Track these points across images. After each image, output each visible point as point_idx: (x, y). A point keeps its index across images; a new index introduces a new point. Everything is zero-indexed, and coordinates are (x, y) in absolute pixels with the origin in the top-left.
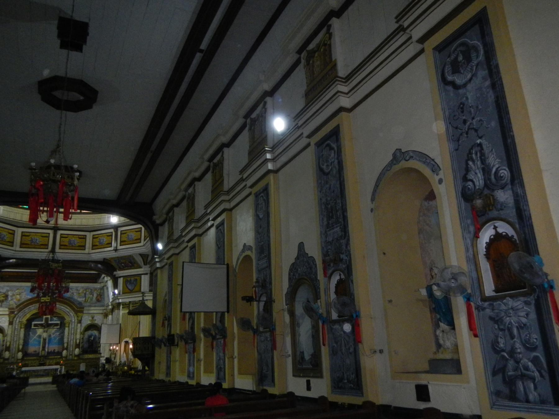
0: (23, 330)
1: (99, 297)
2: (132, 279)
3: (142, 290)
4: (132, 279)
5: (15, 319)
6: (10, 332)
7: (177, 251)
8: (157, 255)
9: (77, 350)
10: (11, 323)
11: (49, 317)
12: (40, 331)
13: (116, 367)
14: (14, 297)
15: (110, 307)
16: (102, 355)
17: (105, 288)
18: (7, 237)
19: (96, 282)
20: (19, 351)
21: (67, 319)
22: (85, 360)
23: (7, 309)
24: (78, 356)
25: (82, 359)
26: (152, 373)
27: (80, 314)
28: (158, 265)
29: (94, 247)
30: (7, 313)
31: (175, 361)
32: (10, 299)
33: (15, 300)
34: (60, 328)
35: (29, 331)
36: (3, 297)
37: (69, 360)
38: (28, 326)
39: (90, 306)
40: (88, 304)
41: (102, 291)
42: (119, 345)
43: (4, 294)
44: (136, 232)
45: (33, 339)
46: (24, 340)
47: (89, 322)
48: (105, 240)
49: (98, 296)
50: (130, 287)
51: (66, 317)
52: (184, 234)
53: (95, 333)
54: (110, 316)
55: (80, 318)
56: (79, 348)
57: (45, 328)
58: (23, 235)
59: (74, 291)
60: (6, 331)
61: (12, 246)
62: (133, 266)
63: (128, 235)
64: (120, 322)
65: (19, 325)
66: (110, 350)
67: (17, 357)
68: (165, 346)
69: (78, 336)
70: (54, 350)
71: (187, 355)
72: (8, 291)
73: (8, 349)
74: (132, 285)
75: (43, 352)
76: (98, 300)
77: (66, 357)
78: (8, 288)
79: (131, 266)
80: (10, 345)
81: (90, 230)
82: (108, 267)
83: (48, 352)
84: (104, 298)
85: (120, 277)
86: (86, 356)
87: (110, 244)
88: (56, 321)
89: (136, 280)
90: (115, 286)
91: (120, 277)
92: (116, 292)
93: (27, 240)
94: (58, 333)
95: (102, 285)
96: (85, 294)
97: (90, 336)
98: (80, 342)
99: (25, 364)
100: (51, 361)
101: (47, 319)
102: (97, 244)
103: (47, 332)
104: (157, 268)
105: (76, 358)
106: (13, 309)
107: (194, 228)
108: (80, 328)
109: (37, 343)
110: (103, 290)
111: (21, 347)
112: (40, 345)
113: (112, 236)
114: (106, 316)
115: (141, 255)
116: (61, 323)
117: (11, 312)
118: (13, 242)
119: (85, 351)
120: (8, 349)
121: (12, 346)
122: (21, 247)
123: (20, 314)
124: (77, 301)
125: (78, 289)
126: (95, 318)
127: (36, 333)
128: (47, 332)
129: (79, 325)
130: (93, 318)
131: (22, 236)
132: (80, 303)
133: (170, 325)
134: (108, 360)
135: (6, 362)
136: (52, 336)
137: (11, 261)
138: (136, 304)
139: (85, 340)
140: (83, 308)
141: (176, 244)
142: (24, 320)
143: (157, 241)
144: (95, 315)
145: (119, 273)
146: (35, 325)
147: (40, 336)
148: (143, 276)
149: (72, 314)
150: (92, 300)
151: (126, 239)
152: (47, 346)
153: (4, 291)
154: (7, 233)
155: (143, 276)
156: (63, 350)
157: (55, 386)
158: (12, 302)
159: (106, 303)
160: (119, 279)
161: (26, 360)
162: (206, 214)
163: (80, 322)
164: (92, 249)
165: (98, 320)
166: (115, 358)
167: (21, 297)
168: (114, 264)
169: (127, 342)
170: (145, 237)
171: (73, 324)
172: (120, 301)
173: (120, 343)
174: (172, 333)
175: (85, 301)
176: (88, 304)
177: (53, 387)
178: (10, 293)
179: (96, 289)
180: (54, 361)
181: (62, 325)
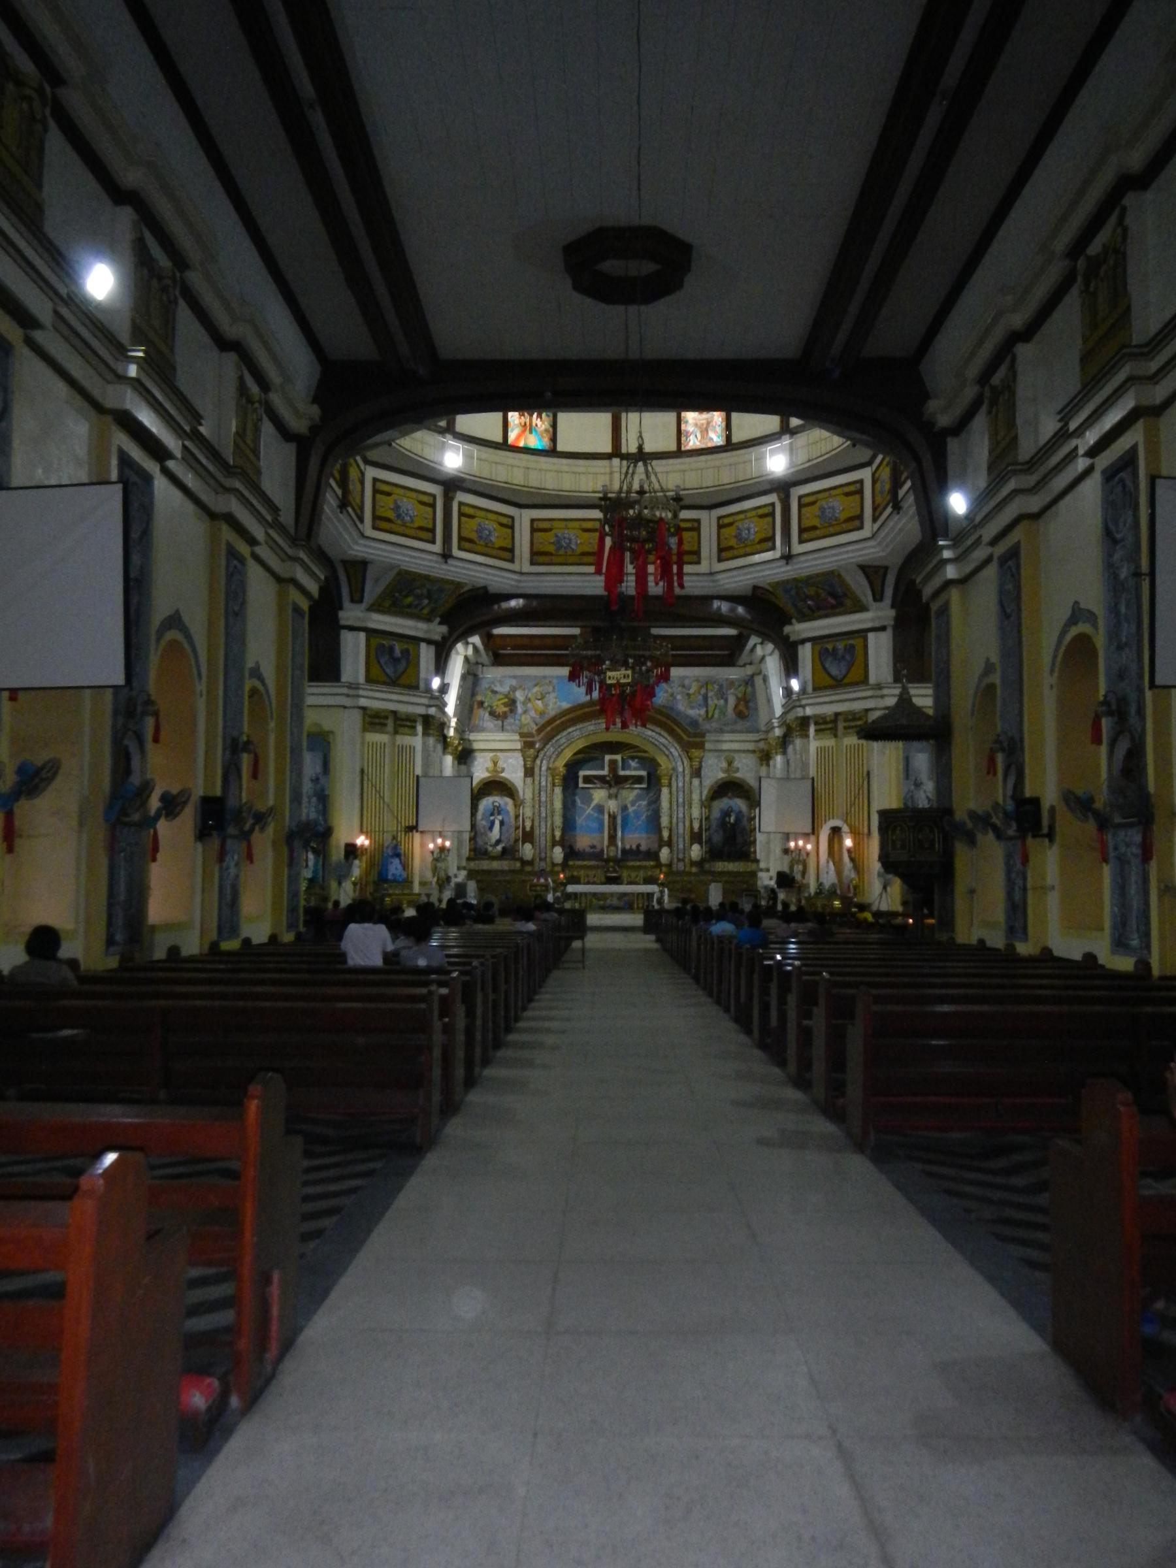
0: (558, 791)
1: (741, 707)
2: (841, 646)
3: (872, 679)
4: (841, 646)
5: (538, 762)
6: (528, 796)
7: (1034, 504)
8: (946, 536)
10: (529, 772)
11: (618, 757)
12: (599, 795)
13: (809, 899)
14: (529, 705)
15: (778, 732)
16: (762, 865)
17: (758, 681)
18: (498, 538)
19: (729, 661)
20: (554, 844)
22: (717, 876)
23: (517, 737)
24: (700, 864)
25: (712, 873)
26: (947, 922)
27: (696, 753)
28: (951, 572)
29: (724, 552)
30: (518, 746)
31: (1044, 889)
32: (520, 709)
33: (532, 713)
34: (648, 789)
35: (574, 794)
36: (505, 705)
37: (679, 873)
38: (570, 781)
39: (721, 731)
40: (714, 725)
41: (749, 689)
42: (813, 838)
43: (506, 696)
44: (847, 494)
45: (584, 815)
47: (721, 775)
48: (755, 529)
49: (739, 700)
50: (834, 671)
51: (661, 760)
52: (1073, 426)
53: (740, 804)
54: (779, 759)
55: (696, 764)
56: (700, 843)
57: (611, 786)
58: (536, 528)
60: (521, 793)
61: (512, 561)
62: (841, 604)
63: (822, 509)
64: (812, 772)
65: (550, 779)
66: (786, 851)
67: (551, 858)
68: (999, 835)
69: (696, 812)
70: (638, 846)
71: (1107, 871)
72: (514, 689)
73: (528, 837)
74: (840, 663)
75: (613, 848)
76: (740, 715)
77: (670, 865)
78: (514, 682)
79: (834, 607)
80: (532, 827)
81: (706, 502)
82: (768, 612)
83: (624, 851)
84: (756, 709)
85: (803, 641)
86: (720, 866)
87: (768, 542)
89: (853, 647)
90: (790, 667)
91: (803, 641)
92: (795, 684)
93: (546, 541)
94: (644, 803)
95: (749, 670)
96: (705, 698)
97: (726, 813)
99: (573, 877)
100: (633, 874)
101: (613, 763)
102: (733, 542)
103: (616, 797)
104: (949, 583)
105: (694, 870)
106: (530, 735)
107: (1131, 380)
108: (699, 791)
109: (595, 825)
110: (753, 686)
111: (558, 834)
112: (602, 832)
113: (772, 514)
114: (765, 757)
115: (863, 568)
116: (649, 775)
117: (528, 745)
118: (511, 550)
119: (714, 854)
120: (528, 837)
121: (537, 832)
122: (532, 563)
123: (550, 749)
124: (688, 716)
125: (687, 682)
126: (736, 764)
127: (589, 799)
128: (616, 797)
129: (696, 782)
130: (730, 763)
131: (533, 530)
132: (694, 723)
133: (1016, 768)
134: (785, 880)
135: (528, 869)
136: (631, 809)
137: (513, 603)
138: (855, 719)
139: (714, 824)
140: (703, 735)
141: (1031, 480)
142: (560, 765)
143: (943, 487)
144: (736, 756)
145: (799, 629)
146: (587, 779)
147: (600, 809)
148: (871, 636)
149: (675, 751)
150: (723, 713)
151: (816, 522)
152: (619, 834)
153: (505, 689)
154: (495, 526)
155: (871, 636)
156: (660, 847)
157: (652, 937)
158: (526, 719)
159: (763, 718)
160: (800, 647)
161: (572, 867)
162: (1063, 435)
163: (697, 773)
164: (720, 560)
165: (746, 769)
166: (804, 873)
167: (546, 705)
168: (784, 601)
169: (836, 831)
170: (875, 509)
171: (681, 778)
172: (809, 711)
173: (814, 831)
174: (1028, 793)
175: (708, 718)
176: (714, 725)
177: (648, 941)
178: (519, 696)
179: (731, 683)
180: (642, 874)
181: (653, 781)
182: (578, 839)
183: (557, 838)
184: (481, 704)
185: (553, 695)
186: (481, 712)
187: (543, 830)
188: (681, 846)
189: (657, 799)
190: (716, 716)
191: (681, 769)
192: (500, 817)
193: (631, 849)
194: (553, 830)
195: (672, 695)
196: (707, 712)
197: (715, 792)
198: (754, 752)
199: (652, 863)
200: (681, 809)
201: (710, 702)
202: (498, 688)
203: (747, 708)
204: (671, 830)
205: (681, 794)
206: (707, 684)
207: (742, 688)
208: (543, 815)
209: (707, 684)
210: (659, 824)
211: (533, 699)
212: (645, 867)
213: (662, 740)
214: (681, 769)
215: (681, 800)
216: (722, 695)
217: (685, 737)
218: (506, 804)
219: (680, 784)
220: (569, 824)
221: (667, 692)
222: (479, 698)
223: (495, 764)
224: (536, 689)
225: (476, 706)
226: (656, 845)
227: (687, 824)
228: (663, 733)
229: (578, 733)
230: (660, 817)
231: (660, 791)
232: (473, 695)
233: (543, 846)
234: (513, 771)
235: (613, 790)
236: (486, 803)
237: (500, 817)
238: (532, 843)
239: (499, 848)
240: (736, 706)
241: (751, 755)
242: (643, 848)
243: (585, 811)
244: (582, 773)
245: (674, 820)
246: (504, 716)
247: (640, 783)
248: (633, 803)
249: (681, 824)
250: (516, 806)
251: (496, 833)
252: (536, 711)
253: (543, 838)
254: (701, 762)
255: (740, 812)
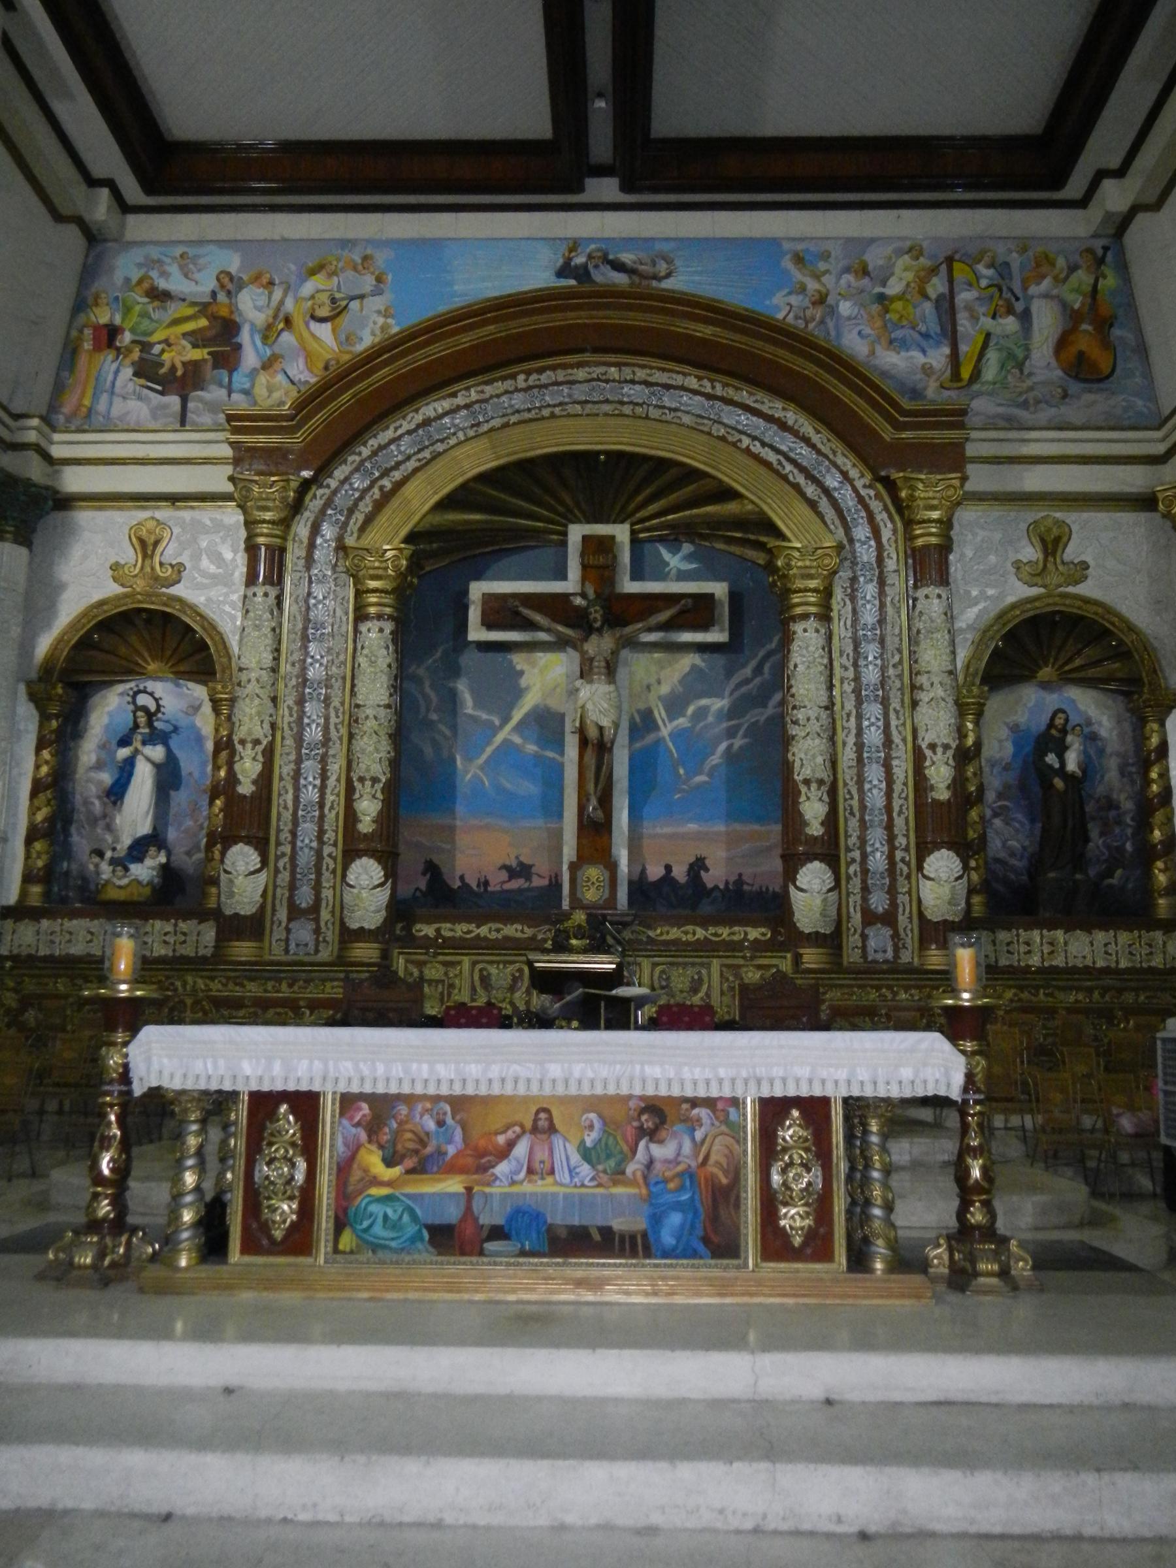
0: (376, 637)
1: (1085, 342)
5: (302, 529)
9: (943, 864)
10: (267, 565)
11: (621, 532)
12: (546, 675)
14: (286, 337)
21: (802, 537)
32: (250, 358)
35: (455, 671)
38: (424, 612)
39: (1012, 424)
41: (1110, 281)
43: (204, 309)
45: (488, 755)
46: (401, 735)
47: (1019, 591)
49: (1073, 318)
53: (1092, 708)
55: (926, 537)
56: (964, 849)
59: (838, 282)
67: (341, 908)
69: (936, 722)
70: (698, 866)
72: (230, 284)
73: (246, 818)
75: (593, 872)
76: (1083, 371)
77: (832, 941)
78: (234, 263)
80: (265, 779)
83: (641, 889)
84: (1142, 350)
88: (677, 573)
94: (718, 704)
95: (1115, 196)
96: (947, 307)
97: (1052, 738)
98: (958, 783)
100: (680, 980)
101: (598, 547)
103: (610, 671)
109: (529, 788)
110: (1123, 267)
111: (369, 808)
116: (735, 597)
121: (283, 797)
123: (349, 478)
125: (874, 258)
126: (1072, 552)
128: (610, 671)
130: (1052, 544)
135: (243, 950)
139: (994, 783)
142: (387, 545)
144: (1074, 518)
147: (546, 724)
149: (846, 478)
150: (1017, 362)
153: (204, 285)
156: (792, 864)
161: (427, 944)
178: (252, 307)
179: (1042, 264)
182: (463, 840)
183: (366, 825)
184: (109, 336)
185: (376, 303)
186: (108, 363)
187: (311, 794)
188: (878, 861)
189: (778, 679)
190: (990, 372)
191: (866, 554)
192: (157, 752)
193: (668, 877)
194: (350, 789)
195: (821, 300)
196: (955, 359)
197: (996, 654)
198: (1146, 502)
199: (754, 933)
200: (873, 710)
201: (964, 323)
202: (175, 283)
203: (1107, 345)
204: (833, 792)
205: (871, 651)
206: (950, 260)
207: (1083, 278)
208: (313, 733)
209: (950, 260)
210: (787, 768)
211: (298, 321)
212: (732, 947)
213: (786, 443)
214: (866, 554)
215: (871, 675)
216: (1006, 298)
217: (888, 433)
218: (196, 709)
219: (869, 616)
220: (417, 779)
221: (802, 289)
222: (103, 316)
223: (146, 547)
224: (308, 288)
225: (87, 346)
226: (777, 864)
227: (902, 768)
228: (791, 416)
229: (461, 419)
230: (787, 741)
231: (787, 639)
232: (80, 305)
233: (305, 858)
234: (210, 574)
235: (599, 645)
236: (109, 708)
237: (157, 752)
238: (261, 845)
239: (144, 871)
240: (1062, 344)
241: (1127, 518)
242: (716, 875)
243: (496, 730)
244: (478, 589)
245: (847, 756)
246: (183, 383)
247: (705, 625)
248: (675, 705)
249: (874, 773)
250: (216, 704)
251: (136, 813)
252: (309, 357)
253: (308, 829)
254: (946, 524)
255: (1092, 737)
